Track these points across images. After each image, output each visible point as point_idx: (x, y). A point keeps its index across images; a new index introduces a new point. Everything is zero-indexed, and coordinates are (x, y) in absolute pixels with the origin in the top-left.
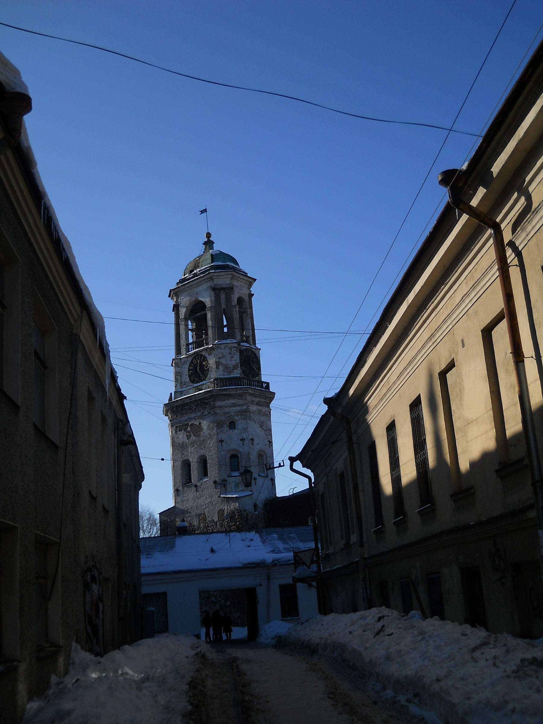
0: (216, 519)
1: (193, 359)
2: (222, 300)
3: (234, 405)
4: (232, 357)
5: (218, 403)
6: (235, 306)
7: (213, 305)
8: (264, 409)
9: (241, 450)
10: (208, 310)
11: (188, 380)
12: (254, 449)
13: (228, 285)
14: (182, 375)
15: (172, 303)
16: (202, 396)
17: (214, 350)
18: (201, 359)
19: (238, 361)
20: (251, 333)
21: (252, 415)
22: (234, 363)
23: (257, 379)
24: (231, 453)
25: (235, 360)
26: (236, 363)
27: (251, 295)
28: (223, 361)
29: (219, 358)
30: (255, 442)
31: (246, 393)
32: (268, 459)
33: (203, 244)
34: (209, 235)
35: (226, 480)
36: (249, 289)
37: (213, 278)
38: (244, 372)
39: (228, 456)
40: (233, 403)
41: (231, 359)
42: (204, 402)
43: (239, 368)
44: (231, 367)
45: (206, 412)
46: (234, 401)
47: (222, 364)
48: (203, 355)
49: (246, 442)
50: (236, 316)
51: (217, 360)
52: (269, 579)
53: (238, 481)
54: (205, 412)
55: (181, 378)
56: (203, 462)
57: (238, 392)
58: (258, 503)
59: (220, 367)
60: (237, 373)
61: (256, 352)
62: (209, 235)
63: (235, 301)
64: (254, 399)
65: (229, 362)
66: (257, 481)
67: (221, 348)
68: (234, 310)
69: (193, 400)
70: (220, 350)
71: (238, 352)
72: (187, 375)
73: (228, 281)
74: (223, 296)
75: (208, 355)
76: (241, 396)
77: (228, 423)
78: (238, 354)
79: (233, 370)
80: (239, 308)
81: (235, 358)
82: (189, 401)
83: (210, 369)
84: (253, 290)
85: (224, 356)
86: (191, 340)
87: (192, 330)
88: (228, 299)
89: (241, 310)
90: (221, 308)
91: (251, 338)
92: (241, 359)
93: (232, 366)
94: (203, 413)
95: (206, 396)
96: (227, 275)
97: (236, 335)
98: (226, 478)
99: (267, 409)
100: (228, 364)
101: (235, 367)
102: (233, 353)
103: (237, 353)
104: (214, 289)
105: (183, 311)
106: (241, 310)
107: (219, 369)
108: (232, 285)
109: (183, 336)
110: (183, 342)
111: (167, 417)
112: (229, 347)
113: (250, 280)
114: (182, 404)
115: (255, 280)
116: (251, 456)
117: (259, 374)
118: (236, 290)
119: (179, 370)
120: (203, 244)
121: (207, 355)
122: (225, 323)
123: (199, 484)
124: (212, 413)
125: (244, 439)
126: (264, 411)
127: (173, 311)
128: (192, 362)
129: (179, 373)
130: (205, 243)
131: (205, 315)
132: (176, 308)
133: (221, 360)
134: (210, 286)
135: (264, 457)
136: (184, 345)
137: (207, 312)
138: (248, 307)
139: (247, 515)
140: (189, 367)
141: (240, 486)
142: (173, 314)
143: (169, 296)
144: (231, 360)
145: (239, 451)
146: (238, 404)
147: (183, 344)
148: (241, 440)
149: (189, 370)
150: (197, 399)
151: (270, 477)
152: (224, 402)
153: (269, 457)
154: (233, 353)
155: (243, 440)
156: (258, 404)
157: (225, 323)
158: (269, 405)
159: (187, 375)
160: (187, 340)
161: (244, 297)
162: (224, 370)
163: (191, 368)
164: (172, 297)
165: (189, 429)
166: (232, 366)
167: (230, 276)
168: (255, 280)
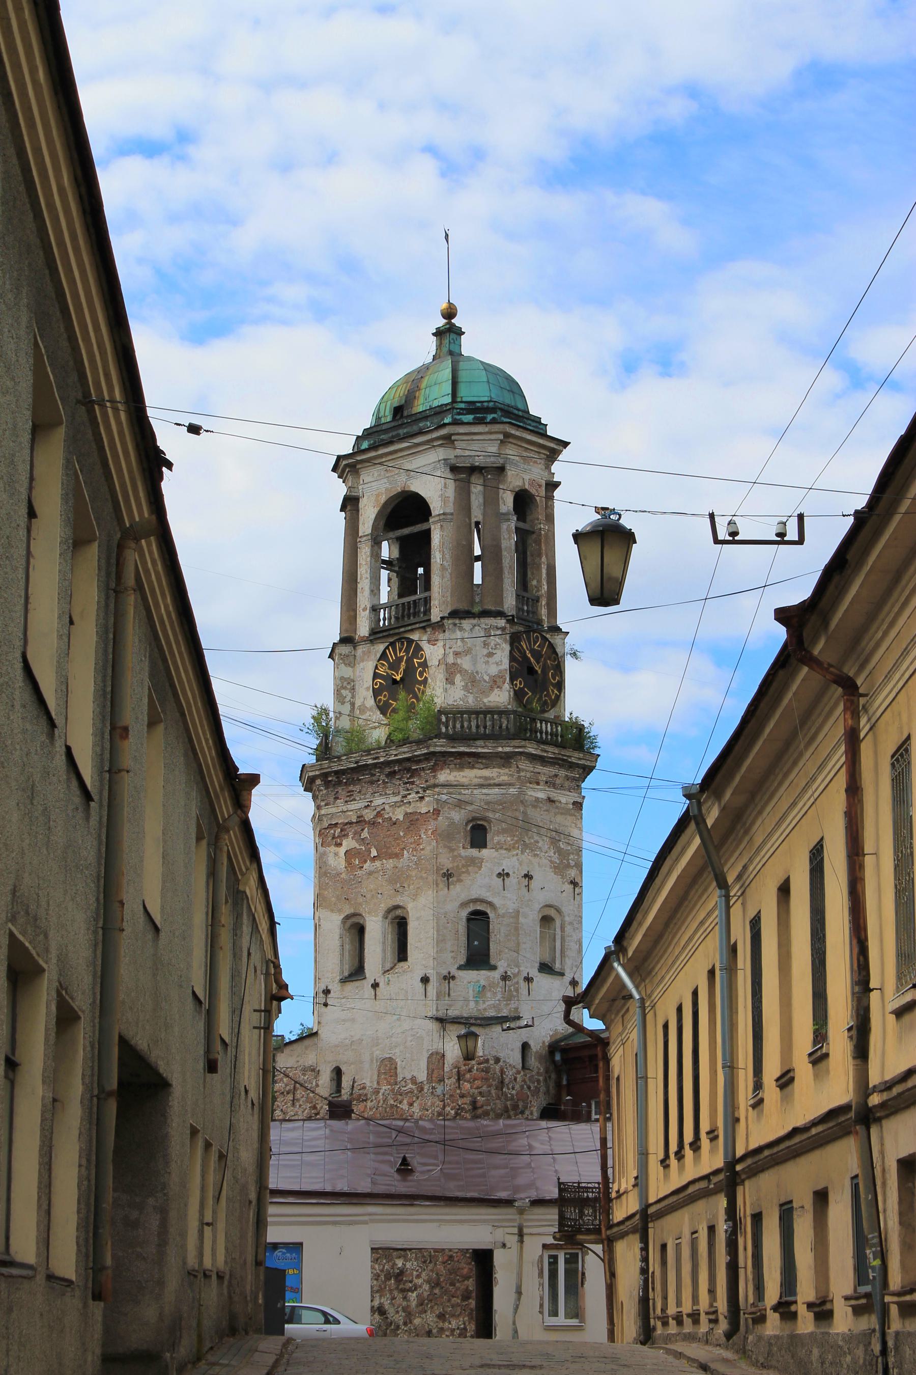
0: (422, 1076)
1: (387, 648)
2: (473, 497)
3: (485, 784)
4: (490, 655)
5: (444, 776)
6: (504, 517)
7: (448, 511)
8: (565, 798)
9: (496, 901)
10: (434, 523)
11: (371, 702)
12: (530, 900)
13: (492, 459)
14: (357, 687)
15: (339, 489)
16: (404, 753)
17: (444, 631)
18: (407, 651)
19: (506, 664)
20: (546, 587)
21: (530, 811)
22: (494, 670)
23: (551, 715)
24: (472, 908)
25: (497, 664)
26: (500, 671)
27: (553, 486)
28: (465, 663)
29: (457, 654)
30: (534, 884)
31: (521, 753)
32: (568, 929)
33: (433, 334)
34: (450, 313)
35: (453, 978)
36: (548, 467)
37: (453, 438)
38: (518, 695)
39: (464, 913)
40: (486, 778)
41: (486, 659)
42: (410, 768)
43: (507, 686)
44: (485, 681)
45: (413, 795)
46: (486, 773)
47: (462, 671)
48: (413, 641)
49: (512, 881)
50: (509, 540)
51: (451, 659)
52: (521, 1235)
53: (483, 983)
54: (410, 794)
55: (353, 697)
56: (401, 926)
57: (500, 749)
58: (532, 1043)
59: (458, 678)
60: (501, 697)
61: (556, 640)
62: (450, 313)
63: (507, 502)
64: (539, 768)
65: (481, 667)
66: (533, 986)
67: (461, 629)
68: (504, 526)
69: (382, 760)
70: (459, 634)
71: (505, 640)
72: (368, 689)
73: (493, 448)
74: (477, 489)
75: (429, 641)
76: (506, 760)
77: (469, 828)
78: (507, 647)
79: (492, 688)
80: (518, 519)
81: (496, 658)
82: (370, 762)
83: (429, 680)
84: (559, 470)
85: (468, 652)
86: (384, 599)
87: (389, 564)
88: (491, 500)
89: (521, 525)
90: (470, 519)
91: (544, 603)
92: (512, 658)
93: (487, 678)
94: (405, 796)
95: (416, 753)
96: (491, 433)
97: (505, 595)
98: (454, 972)
99: (572, 797)
100: (477, 672)
101: (495, 683)
102: (492, 644)
103: (504, 645)
104: (454, 469)
105: (369, 513)
106: (521, 525)
107: (454, 684)
108: (501, 461)
109: (364, 584)
110: (364, 600)
111: (310, 794)
112: (483, 626)
113: (552, 445)
114: (352, 769)
115: (565, 444)
116: (521, 920)
117: (557, 700)
118: (510, 472)
119: (347, 672)
120: (433, 334)
121: (425, 645)
122: (477, 551)
123: (382, 982)
124: (427, 799)
125: (508, 875)
126: (563, 800)
127: (341, 510)
128: (383, 656)
129: (350, 681)
130: (439, 333)
131: (427, 534)
132: (350, 504)
133: (459, 661)
134: (444, 460)
135: (558, 923)
136: (365, 609)
137: (433, 527)
138: (542, 517)
139: (502, 1072)
140: (376, 668)
141: (489, 994)
142: (340, 518)
143: (334, 469)
144: (487, 663)
145: (490, 904)
146: (496, 781)
147: (363, 606)
148: (499, 875)
149: (376, 676)
150: (393, 758)
151: (568, 977)
152: (462, 773)
153: (571, 923)
154: (492, 644)
155: (503, 875)
156: (551, 784)
157: (477, 551)
158: (579, 787)
159: (368, 689)
160: (375, 595)
161: (533, 491)
162: (465, 688)
163: (381, 671)
164: (343, 471)
165: (365, 834)
166: (487, 678)
167: (501, 437)
168: (565, 444)
